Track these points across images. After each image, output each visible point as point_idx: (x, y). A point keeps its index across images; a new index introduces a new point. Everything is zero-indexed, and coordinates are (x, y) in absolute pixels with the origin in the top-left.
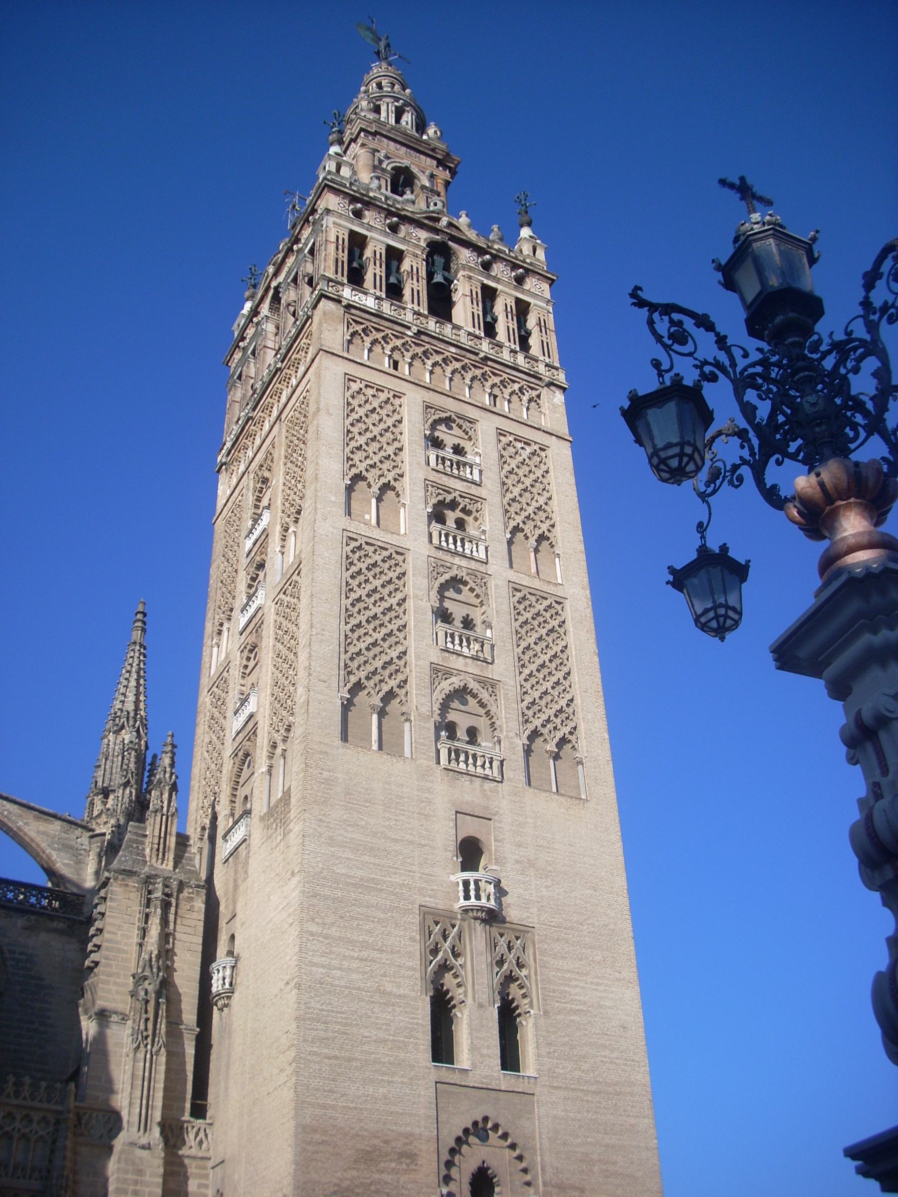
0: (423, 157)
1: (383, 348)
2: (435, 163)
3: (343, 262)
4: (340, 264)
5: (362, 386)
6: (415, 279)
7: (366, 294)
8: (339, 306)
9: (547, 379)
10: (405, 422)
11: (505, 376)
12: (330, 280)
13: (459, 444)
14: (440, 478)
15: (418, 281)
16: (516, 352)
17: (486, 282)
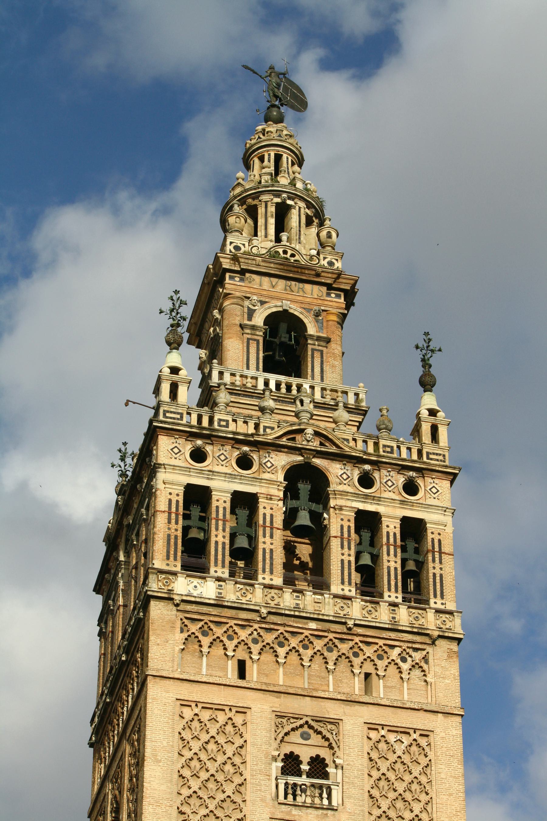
0: (308, 287)
1: (225, 649)
2: (324, 289)
3: (176, 537)
4: (172, 541)
5: (196, 711)
6: (268, 535)
7: (204, 578)
8: (171, 607)
9: (436, 634)
10: (249, 747)
11: (381, 642)
12: (161, 572)
13: (318, 756)
14: (289, 813)
15: (272, 537)
16: (395, 605)
17: (361, 506)
